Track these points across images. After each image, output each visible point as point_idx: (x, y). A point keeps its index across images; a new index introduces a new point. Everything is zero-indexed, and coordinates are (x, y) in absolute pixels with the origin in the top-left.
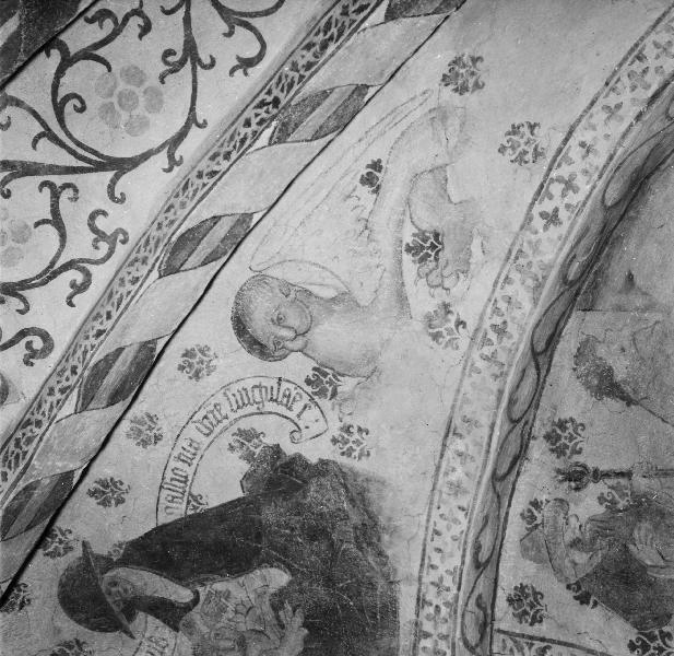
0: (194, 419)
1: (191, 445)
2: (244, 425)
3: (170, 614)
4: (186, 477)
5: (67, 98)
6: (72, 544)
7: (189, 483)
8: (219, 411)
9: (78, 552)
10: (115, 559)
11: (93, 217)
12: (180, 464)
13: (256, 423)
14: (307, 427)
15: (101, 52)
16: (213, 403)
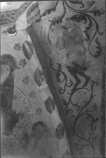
0: (30, 106)
1: (26, 102)
2: (25, 115)
4: (20, 98)
5: (89, 117)
7: (19, 98)
8: (29, 112)
9: (18, 66)
10: (12, 72)
11: (73, 111)
12: (23, 98)
14: (19, 130)
15: (91, 126)
16: (31, 111)
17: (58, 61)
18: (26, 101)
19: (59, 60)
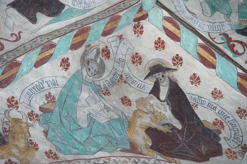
0: (223, 110)
1: (214, 107)
3: (155, 91)
4: (203, 104)
6: (176, 66)
7: (201, 105)
13: (226, 127)
14: (230, 142)
17: (218, 32)
18: (213, 105)
19: (219, 29)
